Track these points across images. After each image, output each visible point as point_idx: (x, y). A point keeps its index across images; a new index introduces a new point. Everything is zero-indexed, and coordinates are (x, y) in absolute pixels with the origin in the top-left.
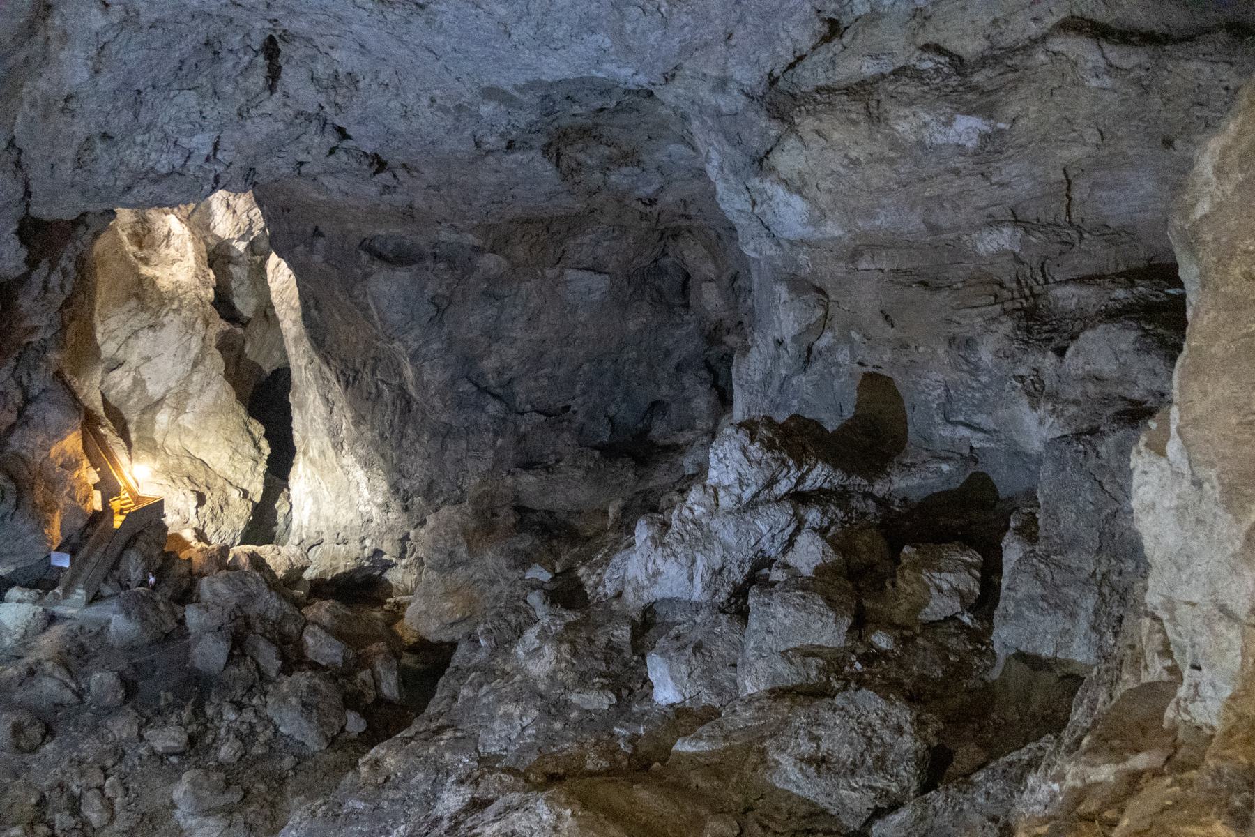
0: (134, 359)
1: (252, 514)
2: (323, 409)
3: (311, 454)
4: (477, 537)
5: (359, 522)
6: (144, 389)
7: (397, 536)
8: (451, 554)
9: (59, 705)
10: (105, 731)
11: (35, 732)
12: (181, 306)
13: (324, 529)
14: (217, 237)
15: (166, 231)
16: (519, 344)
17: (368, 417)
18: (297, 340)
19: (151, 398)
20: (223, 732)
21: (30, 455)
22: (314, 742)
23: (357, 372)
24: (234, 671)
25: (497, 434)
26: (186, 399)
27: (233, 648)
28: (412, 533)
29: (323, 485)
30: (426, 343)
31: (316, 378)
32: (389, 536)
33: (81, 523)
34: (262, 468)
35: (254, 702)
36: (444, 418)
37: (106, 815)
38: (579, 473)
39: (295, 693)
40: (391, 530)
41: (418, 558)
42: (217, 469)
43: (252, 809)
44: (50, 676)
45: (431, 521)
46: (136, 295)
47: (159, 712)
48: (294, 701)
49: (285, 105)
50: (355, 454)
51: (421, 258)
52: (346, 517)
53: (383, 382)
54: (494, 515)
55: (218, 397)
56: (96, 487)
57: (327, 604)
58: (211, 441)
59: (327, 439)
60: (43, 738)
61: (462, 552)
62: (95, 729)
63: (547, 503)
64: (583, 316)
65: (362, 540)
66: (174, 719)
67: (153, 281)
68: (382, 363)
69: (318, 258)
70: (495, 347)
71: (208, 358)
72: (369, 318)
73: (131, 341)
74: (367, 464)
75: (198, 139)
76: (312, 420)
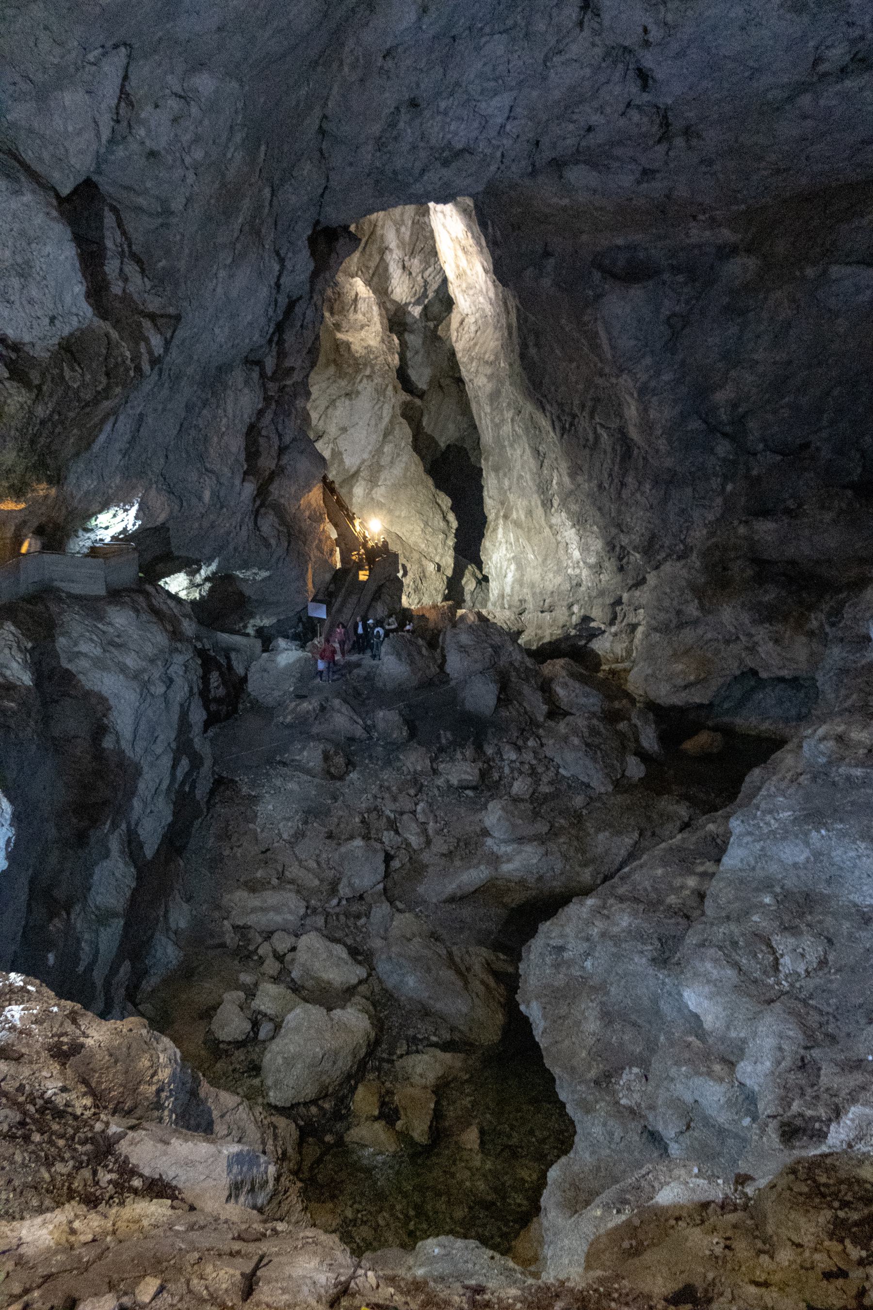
0: (333, 430)
1: (447, 588)
2: (532, 464)
3: (514, 515)
4: (710, 592)
5: (568, 586)
6: (342, 461)
7: (609, 600)
8: (679, 612)
9: (351, 739)
10: (399, 764)
11: (340, 760)
12: (373, 372)
13: (529, 598)
14: (394, 302)
15: (353, 294)
16: (761, 369)
17: (586, 467)
18: (494, 396)
19: (348, 471)
20: (507, 770)
21: (286, 504)
22: (600, 784)
23: (574, 416)
24: (504, 713)
25: (726, 478)
26: (379, 471)
27: (500, 693)
28: (625, 596)
29: (528, 549)
30: (658, 373)
31: (527, 430)
32: (600, 600)
33: (328, 577)
34: (451, 542)
35: (530, 743)
36: (668, 462)
37: (422, 839)
38: (828, 517)
39: (575, 731)
40: (602, 593)
41: (628, 625)
42: (411, 542)
43: (562, 840)
44: (339, 711)
45: (652, 579)
46: (335, 361)
47: (442, 750)
48: (576, 741)
49: (594, 45)
50: (568, 511)
51: (658, 272)
52: (554, 582)
53: (602, 426)
54: (725, 569)
55: (406, 469)
56: (338, 542)
57: (561, 661)
58: (403, 515)
59: (535, 496)
60: (347, 765)
61: (692, 610)
62: (388, 763)
63: (790, 551)
64: (842, 325)
65: (570, 607)
66: (459, 756)
67: (348, 345)
68: (603, 403)
69: (546, 282)
70: (733, 373)
71: (397, 427)
72: (595, 347)
73: (330, 411)
74: (579, 521)
75: (495, 102)
76: (520, 477)
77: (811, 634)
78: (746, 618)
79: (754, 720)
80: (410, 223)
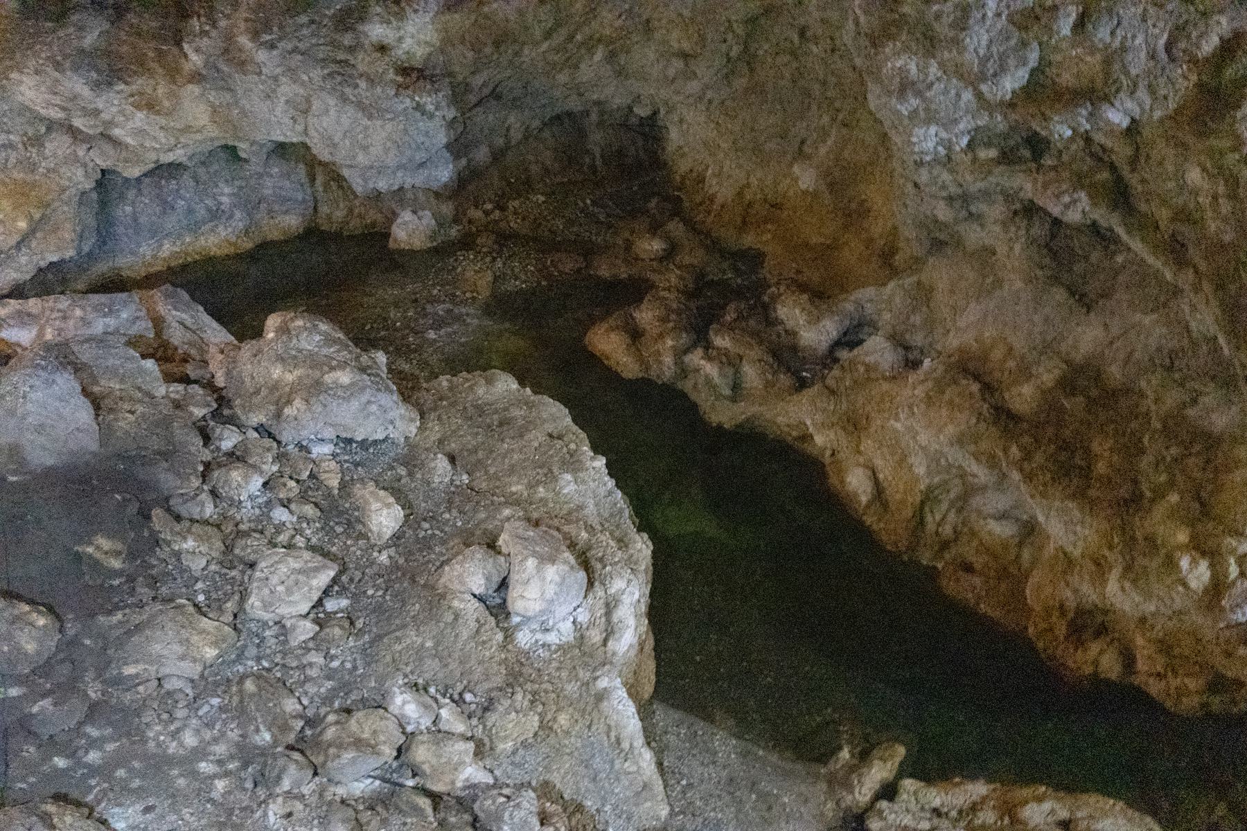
77: (196, 77)
78: (77, 85)
79: (146, 250)
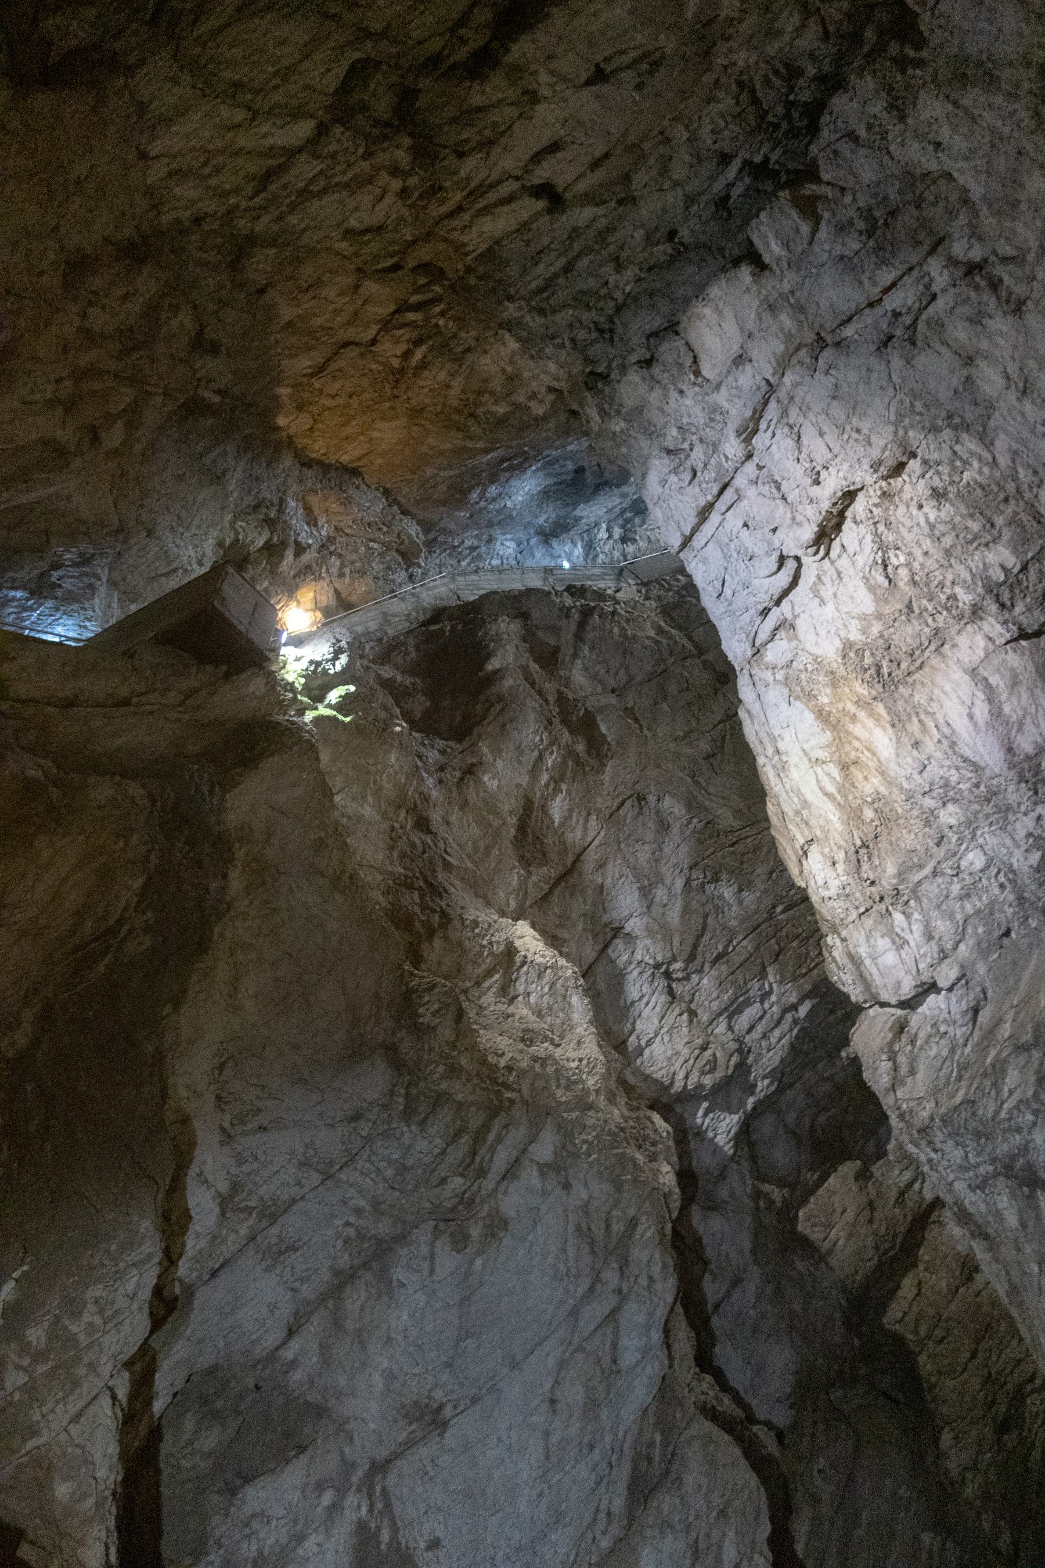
0: (368, 1412)
46: (391, 1051)
71: (693, 1456)
73: (356, 1298)
80: (679, 884)
